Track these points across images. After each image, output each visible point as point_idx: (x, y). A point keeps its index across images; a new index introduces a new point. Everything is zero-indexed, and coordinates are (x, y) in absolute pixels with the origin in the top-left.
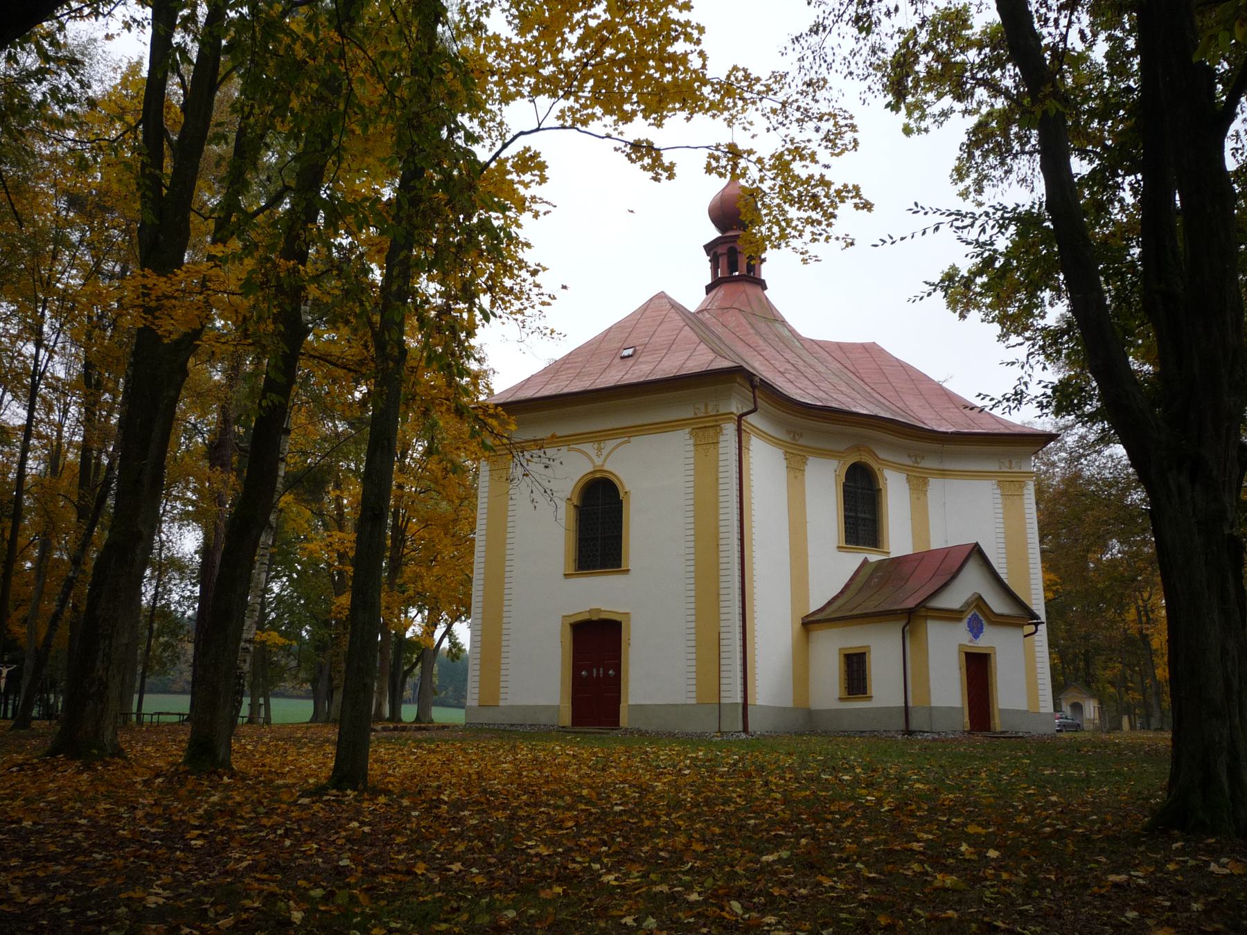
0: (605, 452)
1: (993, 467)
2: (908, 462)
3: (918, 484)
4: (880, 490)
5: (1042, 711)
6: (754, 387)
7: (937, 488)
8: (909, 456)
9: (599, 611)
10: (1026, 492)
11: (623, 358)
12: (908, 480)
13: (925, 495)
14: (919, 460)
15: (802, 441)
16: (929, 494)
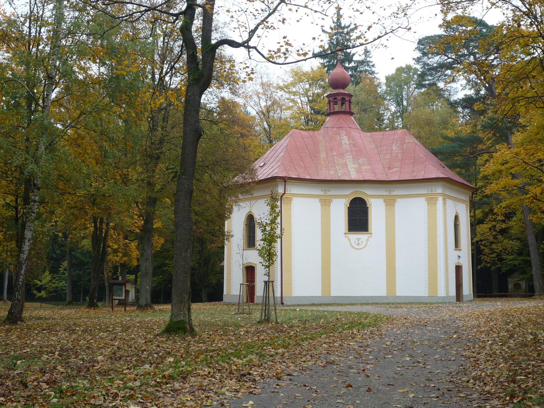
0: (252, 205)
1: (424, 191)
2: (386, 194)
3: (390, 202)
4: (368, 208)
5: (439, 295)
6: (285, 182)
7: (400, 204)
8: (386, 191)
9: (250, 263)
10: (438, 202)
11: (261, 167)
12: (385, 202)
13: (394, 207)
14: (391, 192)
16: (396, 206)
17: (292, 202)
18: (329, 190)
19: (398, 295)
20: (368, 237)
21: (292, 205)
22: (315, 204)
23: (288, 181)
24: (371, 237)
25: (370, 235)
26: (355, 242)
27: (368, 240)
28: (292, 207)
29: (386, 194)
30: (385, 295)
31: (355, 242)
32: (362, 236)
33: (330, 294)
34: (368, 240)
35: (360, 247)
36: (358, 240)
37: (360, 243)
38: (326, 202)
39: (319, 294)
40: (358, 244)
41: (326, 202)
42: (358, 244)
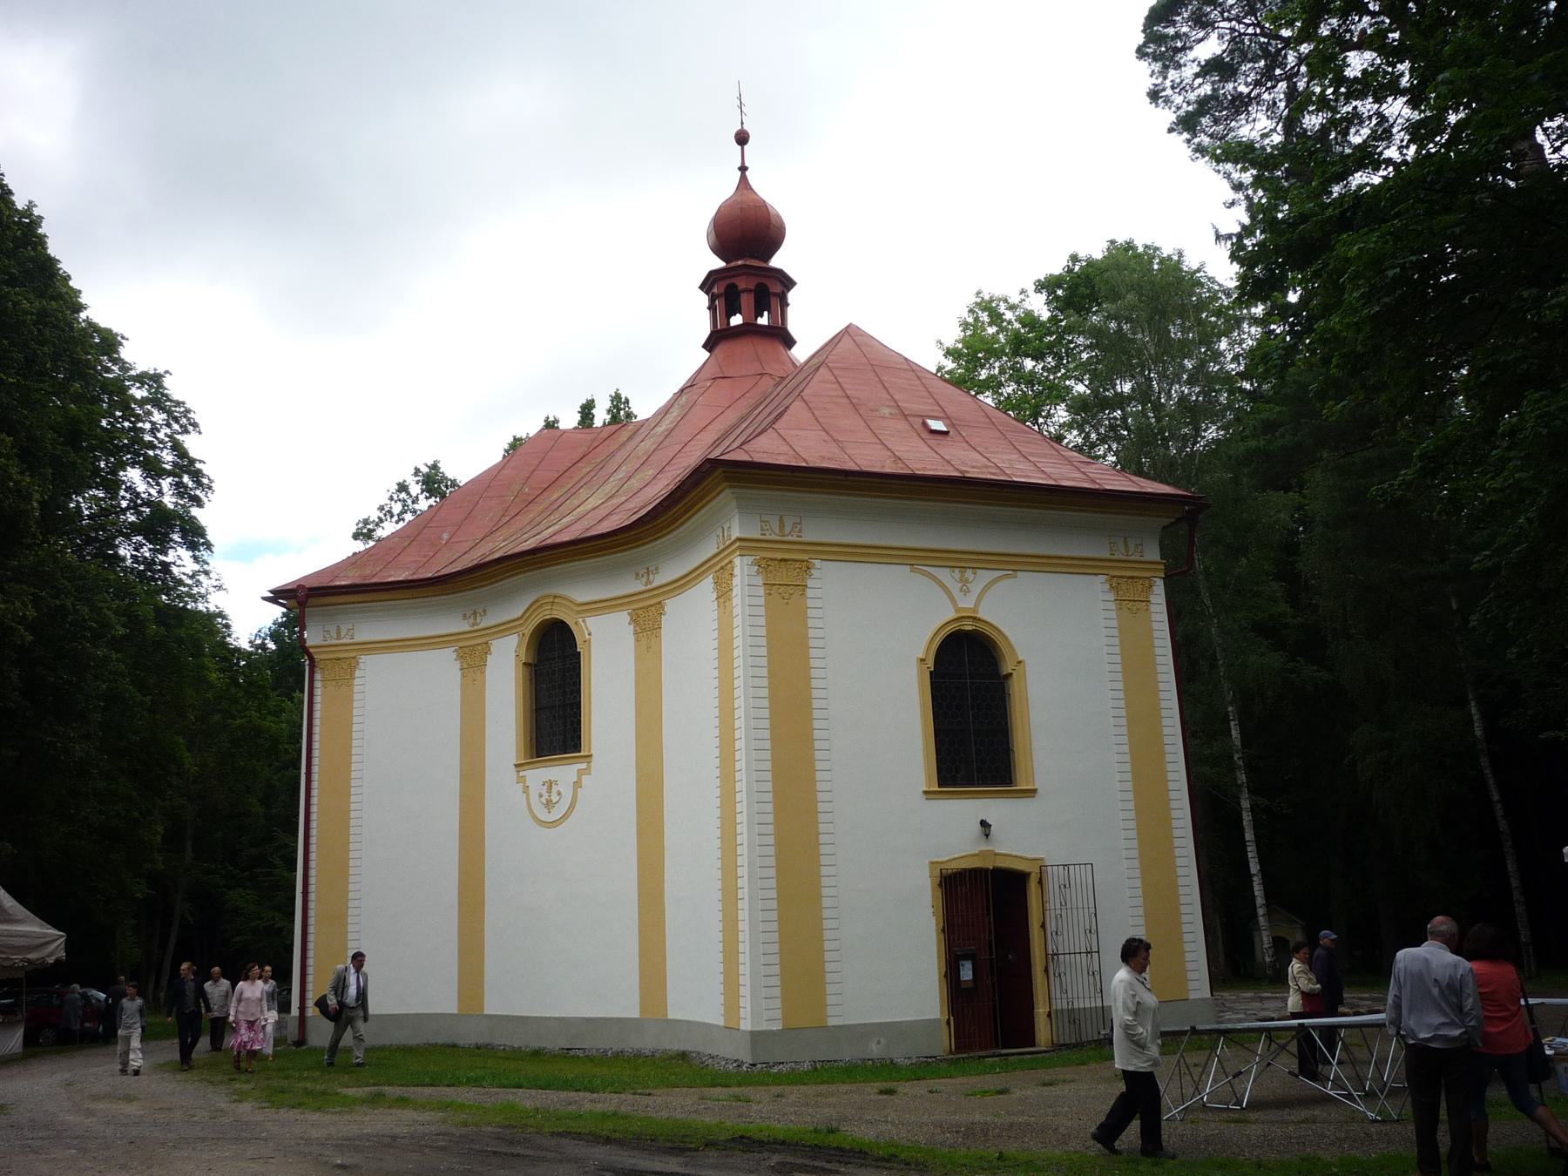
2: (638, 586)
15: (485, 622)
17: (358, 673)
18: (484, 611)
19: (673, 1014)
20: (580, 773)
21: (356, 682)
22: (443, 666)
23: (312, 601)
24: (587, 771)
25: (584, 766)
26: (541, 796)
27: (577, 785)
28: (356, 689)
29: (638, 586)
30: (635, 1014)
31: (541, 796)
32: (562, 772)
33: (481, 1005)
34: (577, 785)
35: (556, 814)
36: (550, 784)
37: (555, 798)
38: (473, 657)
39: (451, 1007)
40: (549, 805)
41: (473, 657)
42: (549, 805)
